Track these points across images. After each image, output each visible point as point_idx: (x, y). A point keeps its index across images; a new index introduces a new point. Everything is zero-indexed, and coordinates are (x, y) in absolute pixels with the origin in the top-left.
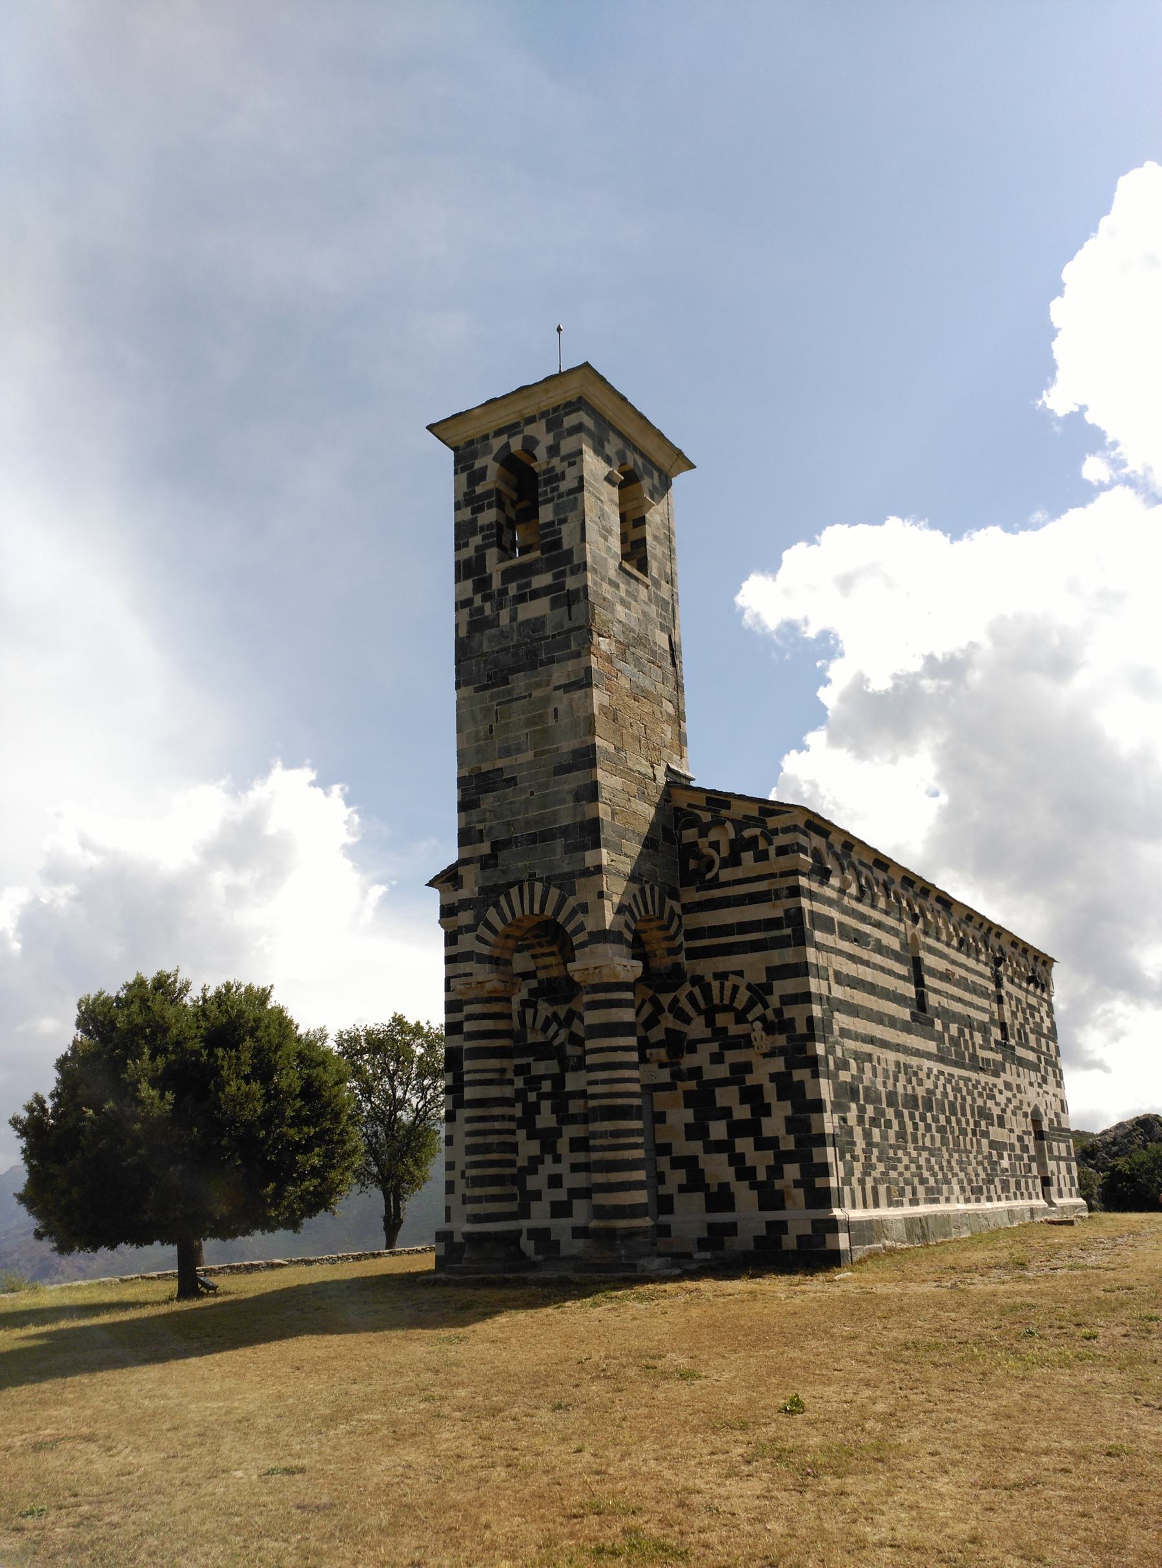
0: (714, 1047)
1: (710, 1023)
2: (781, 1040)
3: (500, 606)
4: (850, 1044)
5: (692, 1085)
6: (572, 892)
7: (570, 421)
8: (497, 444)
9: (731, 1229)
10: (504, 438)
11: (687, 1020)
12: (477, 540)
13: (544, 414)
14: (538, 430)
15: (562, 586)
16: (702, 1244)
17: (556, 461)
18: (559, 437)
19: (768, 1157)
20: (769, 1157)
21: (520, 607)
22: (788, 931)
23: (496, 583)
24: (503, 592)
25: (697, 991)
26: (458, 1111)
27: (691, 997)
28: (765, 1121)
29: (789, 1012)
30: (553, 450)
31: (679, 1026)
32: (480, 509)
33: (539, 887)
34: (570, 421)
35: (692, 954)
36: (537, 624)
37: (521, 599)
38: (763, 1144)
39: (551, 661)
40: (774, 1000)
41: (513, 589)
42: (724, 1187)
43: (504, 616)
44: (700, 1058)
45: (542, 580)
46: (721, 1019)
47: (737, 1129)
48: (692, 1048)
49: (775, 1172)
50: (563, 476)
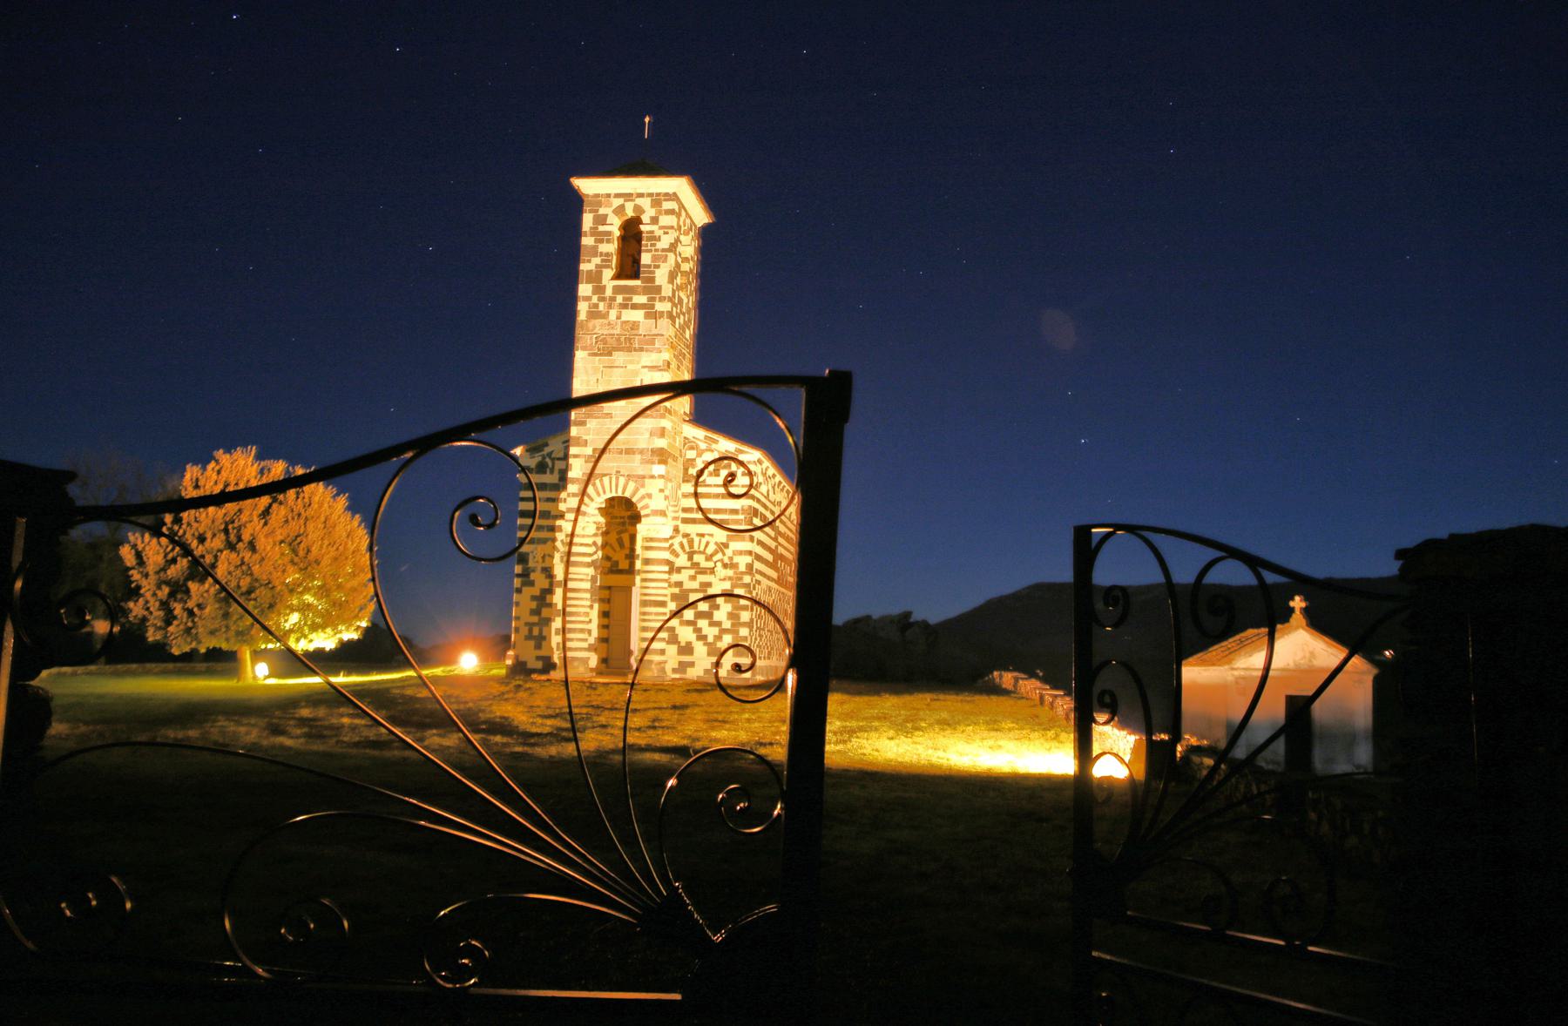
0: (692, 572)
1: (690, 558)
2: (730, 572)
3: (610, 307)
4: (758, 577)
5: (676, 590)
6: (643, 486)
7: (667, 205)
8: (618, 202)
9: (692, 664)
10: (620, 201)
11: (677, 555)
12: (597, 260)
13: (650, 195)
14: (645, 203)
15: (653, 306)
16: (674, 671)
17: (654, 228)
18: (660, 213)
19: (715, 631)
20: (715, 631)
21: (624, 312)
22: (741, 517)
23: (609, 292)
24: (613, 299)
25: (685, 541)
26: (525, 589)
27: (682, 545)
28: (716, 613)
29: (736, 559)
30: (654, 220)
31: (672, 558)
32: (601, 241)
33: (622, 480)
34: (667, 205)
35: (685, 521)
36: (635, 325)
37: (624, 306)
38: (713, 624)
39: (641, 350)
40: (729, 552)
41: (620, 299)
42: (689, 644)
43: (613, 314)
44: (683, 576)
45: (641, 299)
46: (697, 558)
47: (700, 615)
48: (679, 570)
49: (718, 638)
50: (659, 239)
